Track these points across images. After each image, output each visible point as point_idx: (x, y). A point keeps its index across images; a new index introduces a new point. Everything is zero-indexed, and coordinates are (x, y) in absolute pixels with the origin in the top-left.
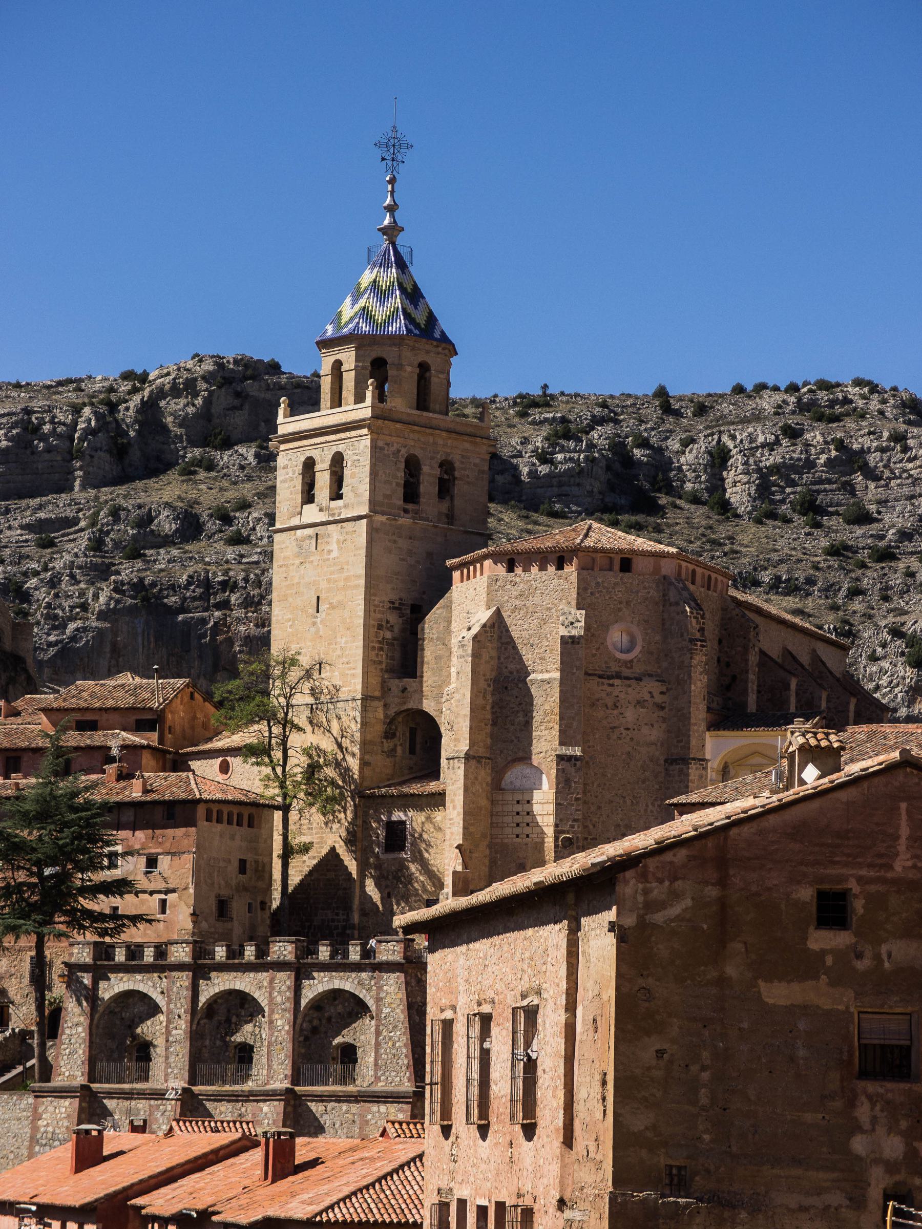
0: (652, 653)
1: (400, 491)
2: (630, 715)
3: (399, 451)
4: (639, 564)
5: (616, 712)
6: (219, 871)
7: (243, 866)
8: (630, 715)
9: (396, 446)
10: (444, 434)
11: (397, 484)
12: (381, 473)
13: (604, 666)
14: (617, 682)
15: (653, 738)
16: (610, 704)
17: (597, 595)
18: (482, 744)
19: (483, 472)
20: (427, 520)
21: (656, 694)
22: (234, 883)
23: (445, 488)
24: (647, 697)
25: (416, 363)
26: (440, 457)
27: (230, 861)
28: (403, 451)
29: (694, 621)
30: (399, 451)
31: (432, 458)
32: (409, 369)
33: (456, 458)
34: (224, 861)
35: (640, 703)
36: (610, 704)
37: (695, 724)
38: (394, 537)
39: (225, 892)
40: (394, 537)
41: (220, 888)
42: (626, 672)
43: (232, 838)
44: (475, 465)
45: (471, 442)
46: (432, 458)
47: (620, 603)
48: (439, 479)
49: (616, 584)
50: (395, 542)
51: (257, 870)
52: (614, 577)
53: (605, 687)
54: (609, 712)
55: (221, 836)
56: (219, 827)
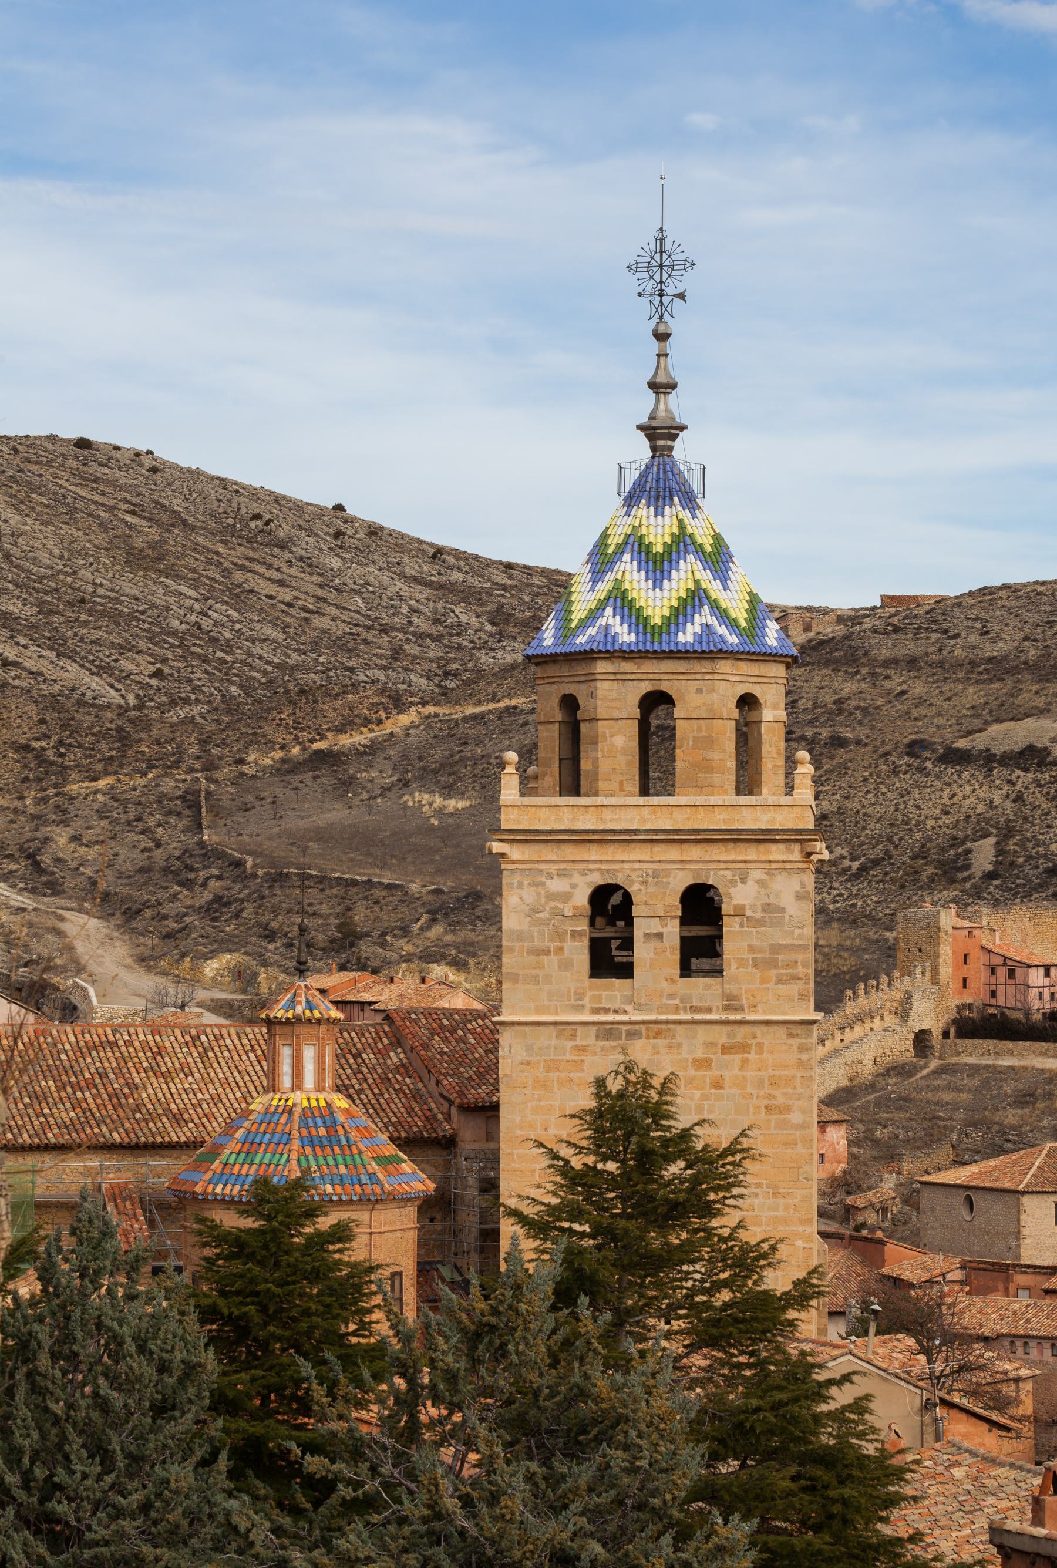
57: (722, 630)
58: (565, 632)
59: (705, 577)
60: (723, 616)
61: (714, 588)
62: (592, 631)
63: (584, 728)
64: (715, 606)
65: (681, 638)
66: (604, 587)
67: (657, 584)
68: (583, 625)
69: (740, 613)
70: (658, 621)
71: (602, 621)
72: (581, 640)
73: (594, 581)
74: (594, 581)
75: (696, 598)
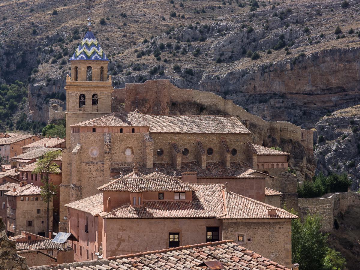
0: (102, 155)
1: (78, 105)
2: (94, 173)
3: (77, 94)
4: (98, 130)
5: (90, 173)
6: (28, 214)
7: (39, 211)
8: (94, 173)
9: (76, 92)
10: (93, 87)
11: (77, 103)
12: (70, 101)
13: (88, 159)
14: (90, 164)
15: (101, 180)
16: (89, 171)
17: (86, 139)
18: (67, 181)
19: (109, 96)
20: (88, 112)
21: (101, 167)
22: (35, 216)
23: (95, 102)
24: (99, 168)
25: (86, 67)
26: (92, 94)
27: (33, 211)
28: (79, 94)
29: (106, 147)
30: (77, 94)
31: (89, 94)
32: (83, 69)
33: (98, 93)
34: (30, 211)
35: (97, 170)
36: (89, 171)
37: (106, 177)
38: (76, 118)
39: (30, 219)
40: (76, 118)
41: (28, 218)
42: (94, 161)
43: (33, 204)
44: (106, 94)
45: (104, 88)
46: (89, 94)
47: (93, 141)
48: (93, 100)
49: (91, 136)
50: (76, 119)
51: (45, 212)
52: (91, 134)
53: (88, 166)
54: (88, 173)
55: (28, 204)
56: (27, 202)
57: (99, 57)
58: (76, 57)
59: (96, 49)
60: (99, 55)
61: (97, 51)
62: (80, 57)
63: (79, 71)
64: (97, 53)
65: (93, 58)
66: (81, 51)
67: (89, 50)
68: (78, 56)
69: (101, 54)
70: (89, 56)
71: (81, 56)
72: (78, 58)
73: (80, 50)
74: (80, 50)
75: (95, 52)
